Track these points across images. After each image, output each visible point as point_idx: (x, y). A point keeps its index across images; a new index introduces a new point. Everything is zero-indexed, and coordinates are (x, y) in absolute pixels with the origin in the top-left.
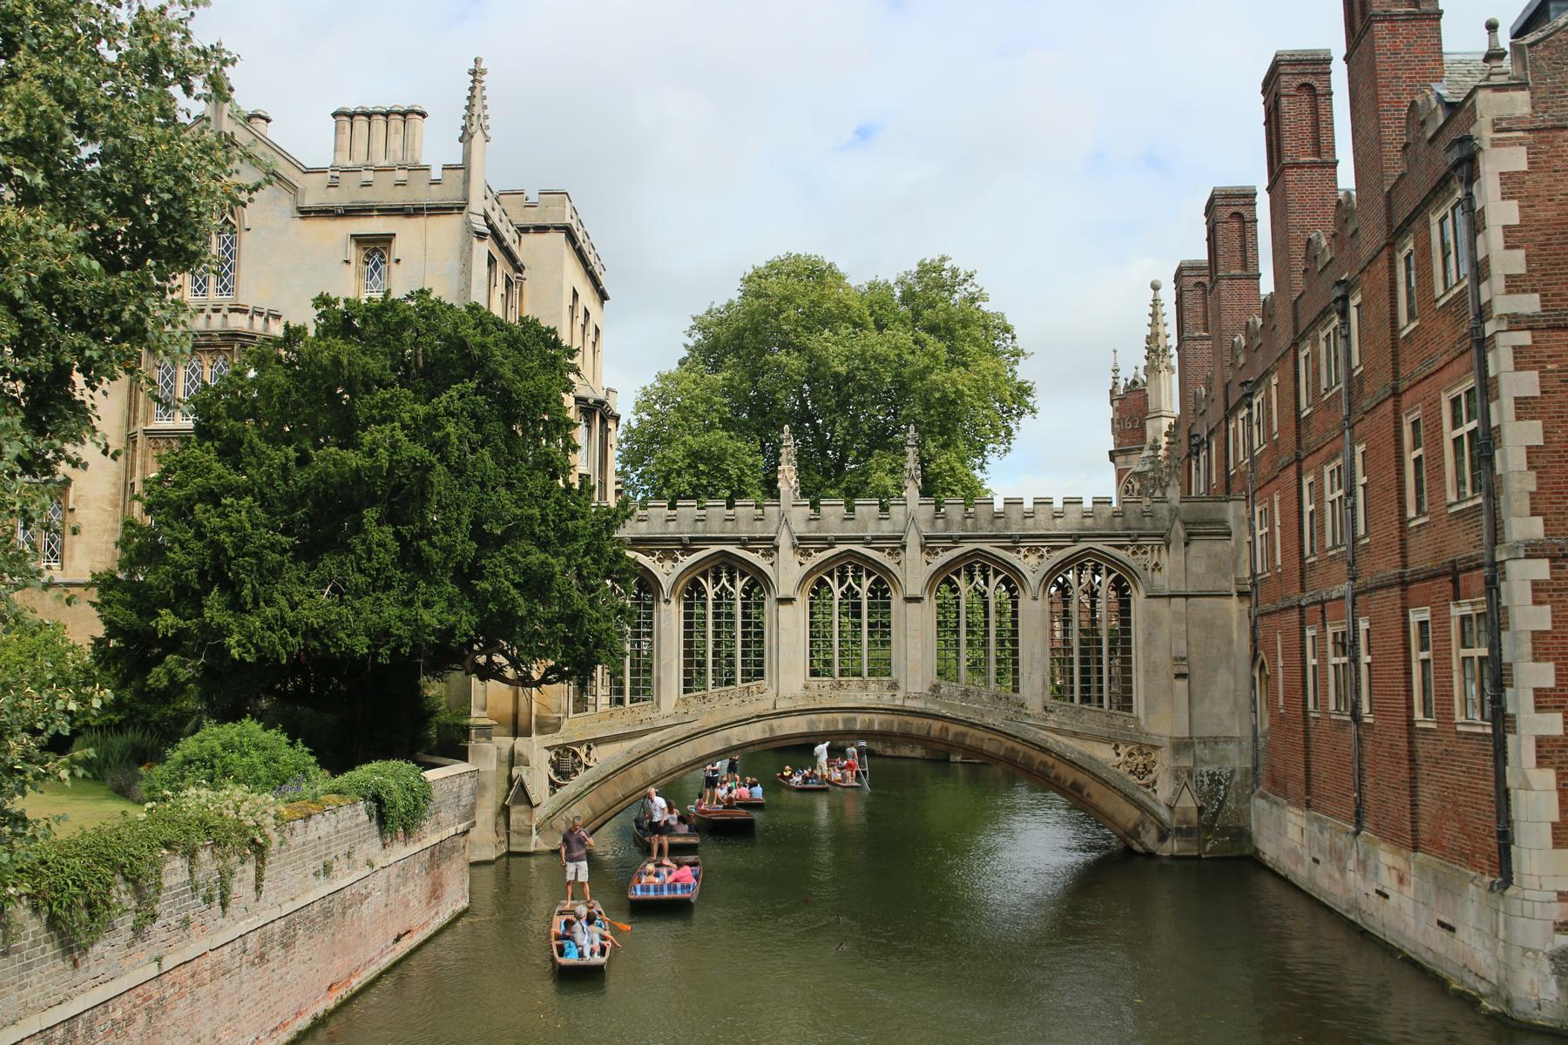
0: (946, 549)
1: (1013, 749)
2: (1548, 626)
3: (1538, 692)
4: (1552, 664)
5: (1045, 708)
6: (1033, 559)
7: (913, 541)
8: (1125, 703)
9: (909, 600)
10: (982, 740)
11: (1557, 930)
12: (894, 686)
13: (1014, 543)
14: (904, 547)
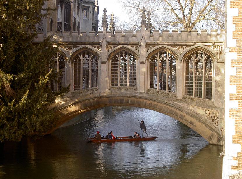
0: (153, 47)
1: (172, 110)
2: (235, 74)
3: (231, 95)
4: (235, 86)
5: (183, 98)
6: (181, 50)
7: (143, 44)
8: (209, 95)
9: (142, 62)
10: (162, 107)
11: (232, 168)
12: (136, 89)
13: (175, 44)
14: (140, 46)
